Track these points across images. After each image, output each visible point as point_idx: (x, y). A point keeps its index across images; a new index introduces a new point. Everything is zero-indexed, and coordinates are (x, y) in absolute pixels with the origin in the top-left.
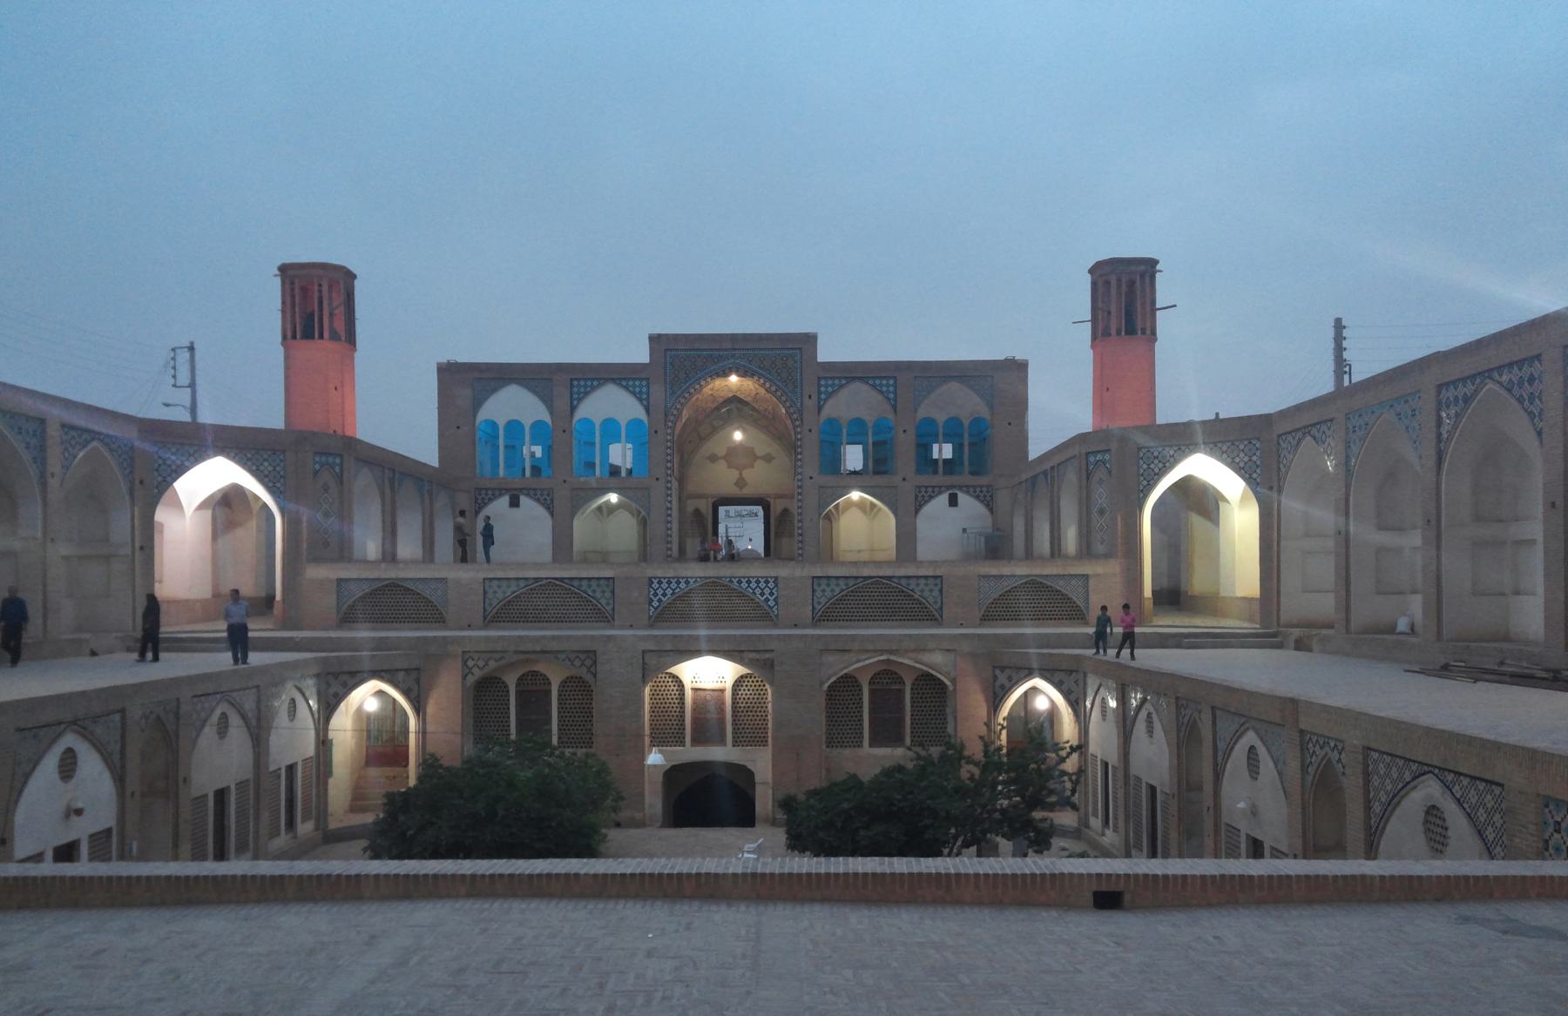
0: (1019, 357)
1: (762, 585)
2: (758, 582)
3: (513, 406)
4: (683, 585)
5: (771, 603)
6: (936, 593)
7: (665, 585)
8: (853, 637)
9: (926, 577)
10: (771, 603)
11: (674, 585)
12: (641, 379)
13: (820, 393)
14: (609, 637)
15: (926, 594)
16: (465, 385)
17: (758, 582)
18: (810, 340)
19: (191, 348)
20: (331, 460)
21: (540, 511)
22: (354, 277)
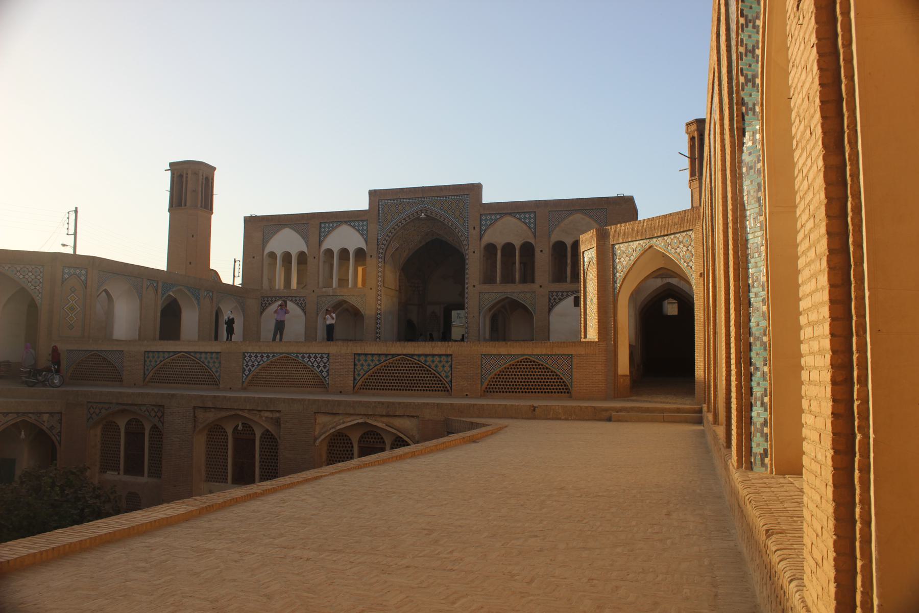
0: (627, 194)
1: (319, 360)
2: (316, 357)
3: (287, 242)
4: (265, 359)
5: (325, 374)
6: (447, 368)
7: (253, 359)
8: (339, 403)
9: (440, 355)
10: (325, 374)
11: (259, 359)
12: (363, 221)
13: (481, 225)
14: (173, 395)
15: (440, 369)
16: (259, 229)
17: (316, 357)
18: (476, 189)
19: (76, 211)
20: (78, 271)
21: (299, 311)
22: (215, 169)
